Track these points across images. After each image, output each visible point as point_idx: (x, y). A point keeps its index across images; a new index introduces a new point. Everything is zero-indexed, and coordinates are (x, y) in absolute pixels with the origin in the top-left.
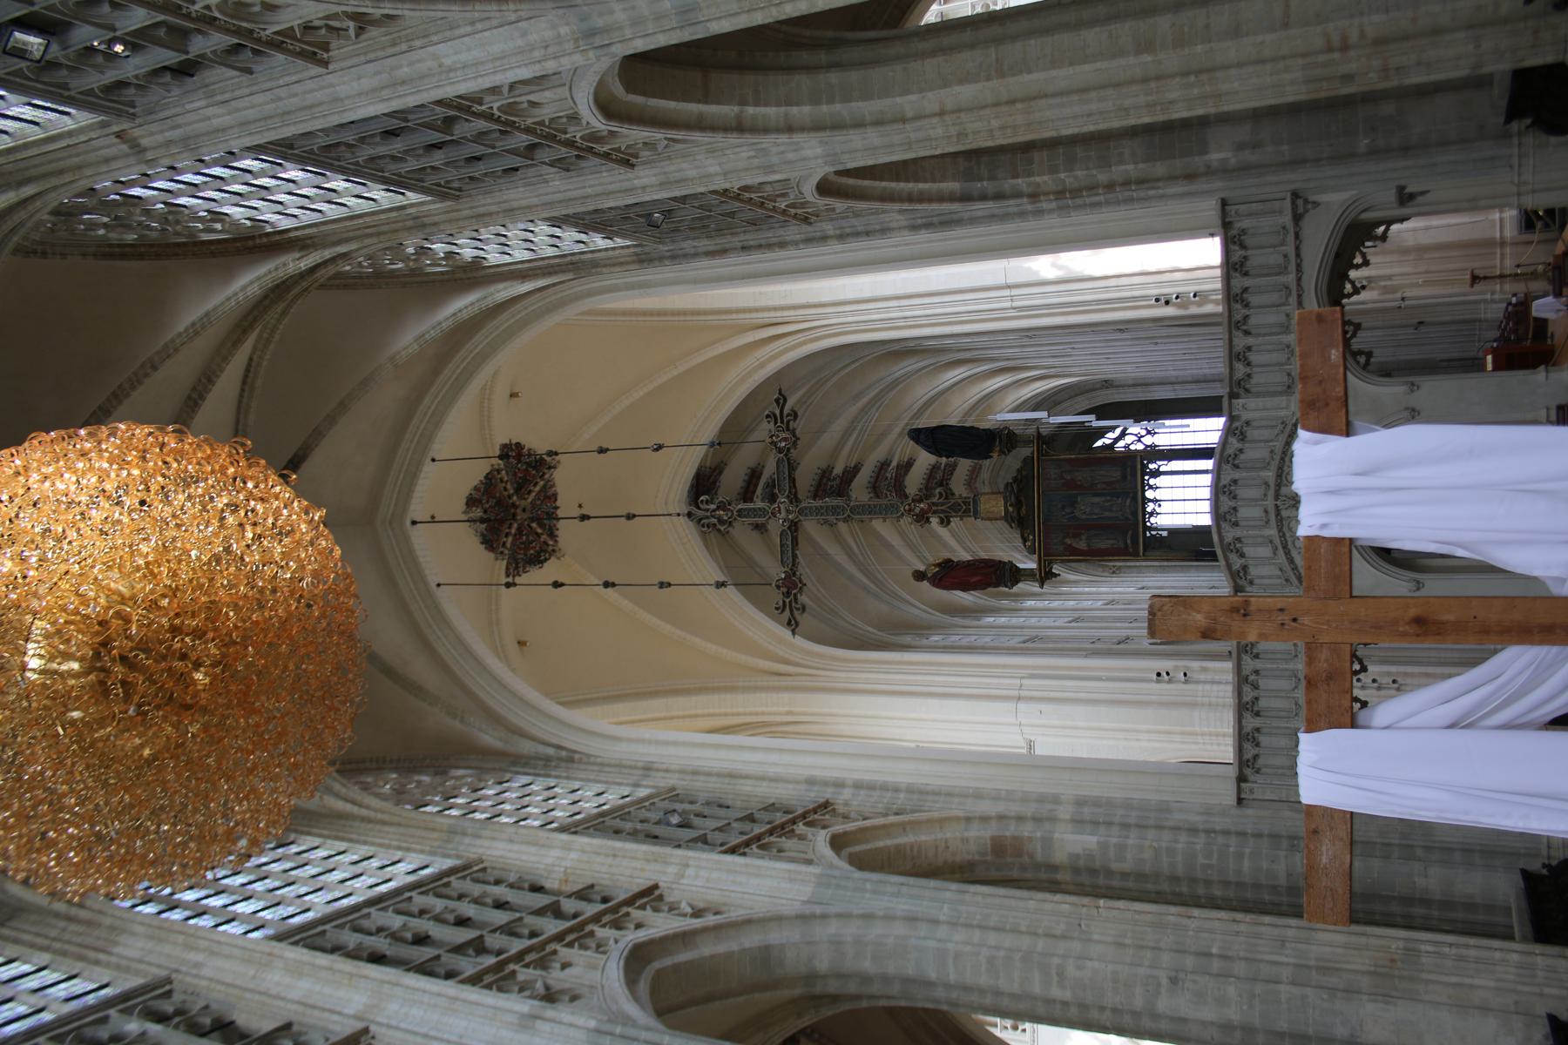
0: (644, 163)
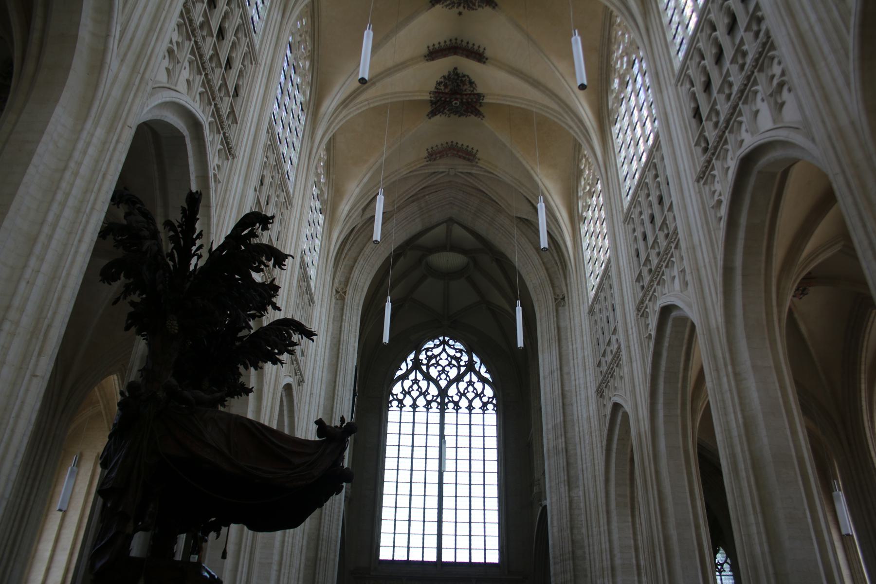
0: (699, 188)
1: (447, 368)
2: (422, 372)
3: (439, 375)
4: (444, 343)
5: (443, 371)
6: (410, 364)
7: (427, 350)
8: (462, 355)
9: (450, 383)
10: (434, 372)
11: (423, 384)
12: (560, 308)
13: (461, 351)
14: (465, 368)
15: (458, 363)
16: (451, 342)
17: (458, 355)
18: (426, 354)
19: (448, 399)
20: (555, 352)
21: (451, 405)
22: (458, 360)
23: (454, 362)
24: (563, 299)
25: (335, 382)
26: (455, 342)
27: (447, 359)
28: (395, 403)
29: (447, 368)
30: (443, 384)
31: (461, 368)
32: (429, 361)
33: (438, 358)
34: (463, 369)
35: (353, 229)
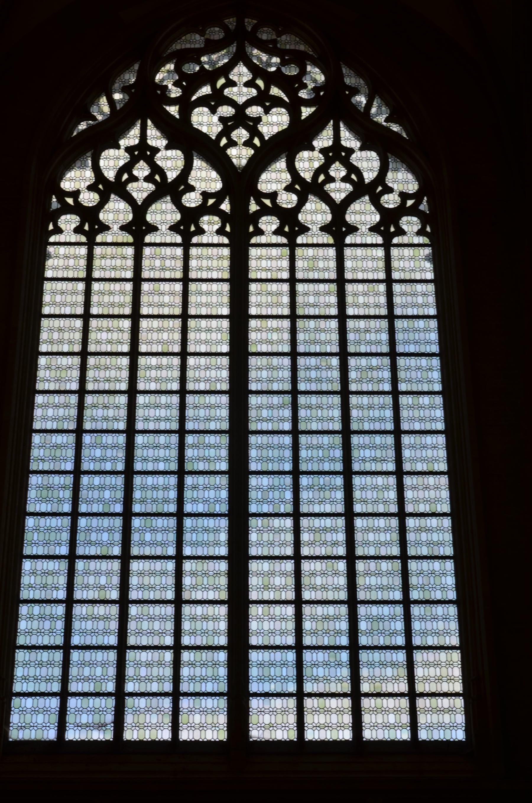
3: (226, 132)
8: (303, 72)
15: (292, 92)
17: (292, 71)
18: (178, 69)
19: (259, 202)
23: (275, 91)
26: (279, 35)
27: (249, 84)
29: (254, 111)
31: (303, 109)
32: (188, 91)
33: (221, 82)
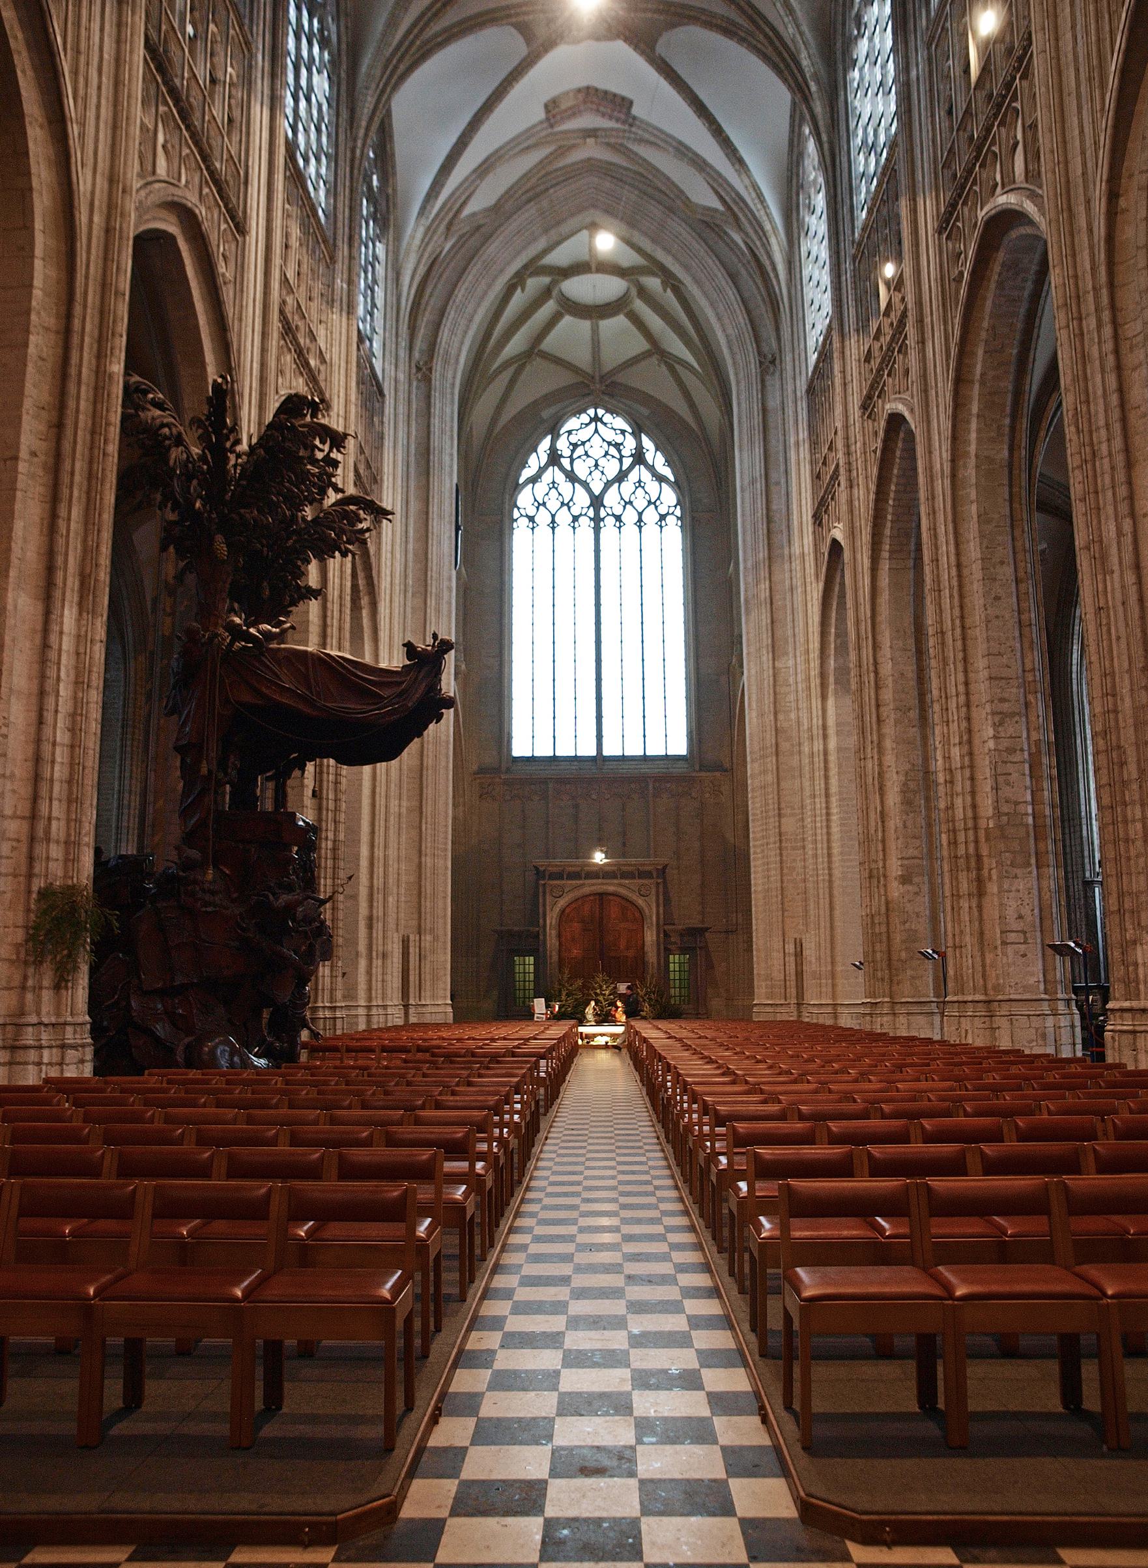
1: (602, 462)
2: (562, 468)
4: (596, 419)
5: (596, 465)
6: (544, 459)
7: (570, 432)
9: (608, 485)
10: (581, 469)
11: (566, 487)
12: (768, 377)
13: (623, 432)
14: (631, 459)
15: (619, 451)
16: (608, 418)
20: (758, 451)
21: (610, 521)
22: (617, 446)
23: (613, 451)
24: (773, 362)
25: (427, 513)
28: (523, 522)
30: (597, 488)
32: (573, 451)
33: (587, 445)
34: (627, 462)
35: (435, 259)
